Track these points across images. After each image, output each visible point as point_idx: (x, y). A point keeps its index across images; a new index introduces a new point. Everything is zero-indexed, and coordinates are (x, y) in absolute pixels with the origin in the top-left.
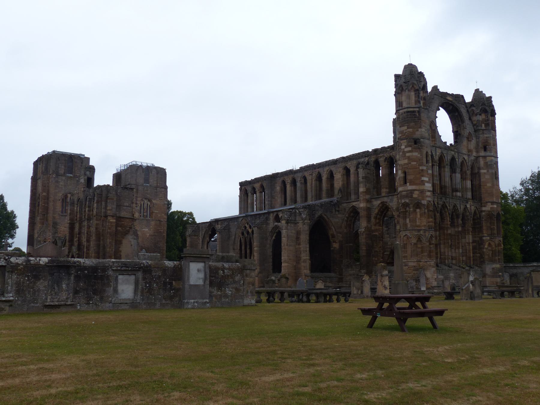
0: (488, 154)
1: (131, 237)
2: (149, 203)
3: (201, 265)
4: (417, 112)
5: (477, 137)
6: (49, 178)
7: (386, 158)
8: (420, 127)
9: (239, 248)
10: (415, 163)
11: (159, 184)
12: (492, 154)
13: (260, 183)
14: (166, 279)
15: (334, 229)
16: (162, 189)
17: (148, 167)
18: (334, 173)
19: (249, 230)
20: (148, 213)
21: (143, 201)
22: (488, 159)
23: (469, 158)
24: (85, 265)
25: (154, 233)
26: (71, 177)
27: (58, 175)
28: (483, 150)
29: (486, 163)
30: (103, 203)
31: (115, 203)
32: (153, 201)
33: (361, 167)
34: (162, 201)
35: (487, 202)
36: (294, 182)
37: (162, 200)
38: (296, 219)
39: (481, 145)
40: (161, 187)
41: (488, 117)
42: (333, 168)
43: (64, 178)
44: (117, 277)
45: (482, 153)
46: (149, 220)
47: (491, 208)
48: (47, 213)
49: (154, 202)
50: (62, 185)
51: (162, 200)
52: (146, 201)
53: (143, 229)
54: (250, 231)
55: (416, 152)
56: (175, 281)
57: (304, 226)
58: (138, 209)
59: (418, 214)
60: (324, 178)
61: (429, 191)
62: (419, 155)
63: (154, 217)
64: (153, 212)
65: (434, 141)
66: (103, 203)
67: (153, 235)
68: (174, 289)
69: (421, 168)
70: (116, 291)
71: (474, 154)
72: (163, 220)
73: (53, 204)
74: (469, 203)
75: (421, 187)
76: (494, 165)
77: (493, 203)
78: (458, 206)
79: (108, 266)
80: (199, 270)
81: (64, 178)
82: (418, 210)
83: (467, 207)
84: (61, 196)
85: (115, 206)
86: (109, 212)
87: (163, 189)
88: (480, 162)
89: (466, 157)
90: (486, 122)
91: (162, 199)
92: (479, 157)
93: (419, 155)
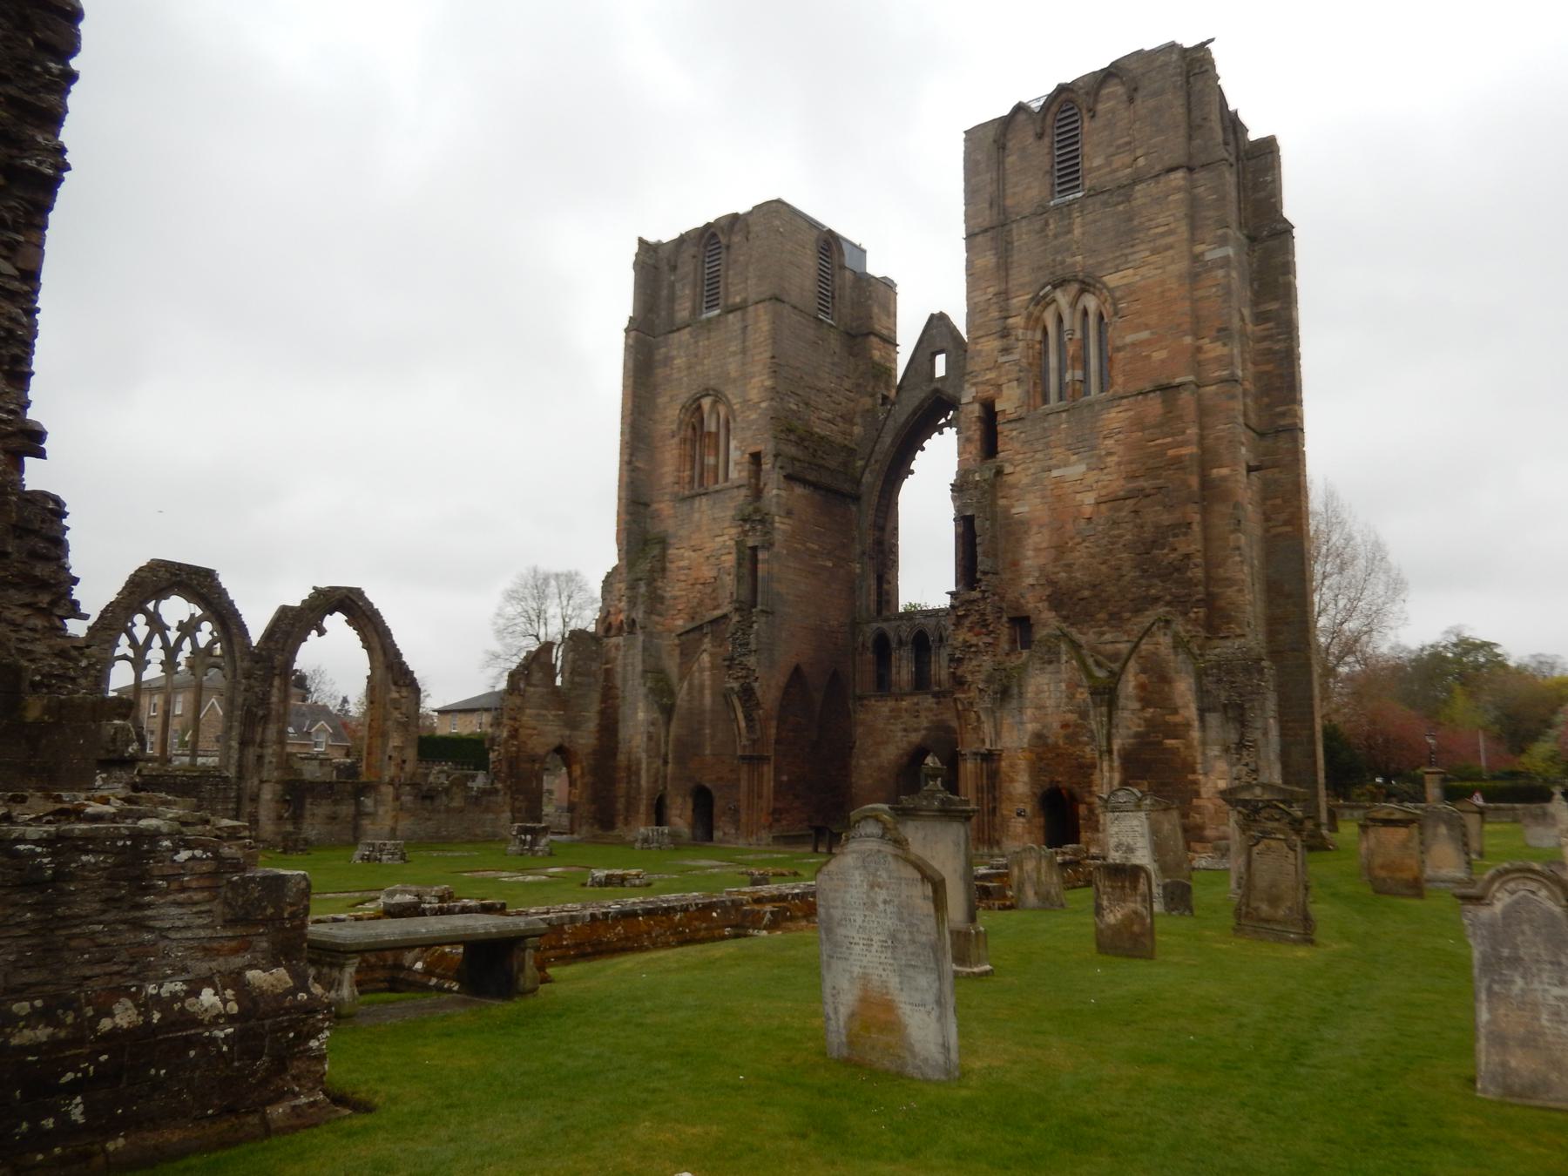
2: (1091, 302)
11: (1145, 155)
16: (1163, 179)
17: (1064, 95)
21: (1052, 308)
26: (709, 320)
32: (1112, 280)
34: (1171, 253)
37: (1169, 247)
40: (1158, 168)
43: (685, 335)
49: (1111, 285)
51: (1169, 247)
52: (1063, 299)
53: (1055, 473)
58: (1016, 362)
63: (1120, 380)
67: (1122, 493)
72: (1191, 378)
81: (688, 336)
87: (1172, 176)
91: (1170, 240)
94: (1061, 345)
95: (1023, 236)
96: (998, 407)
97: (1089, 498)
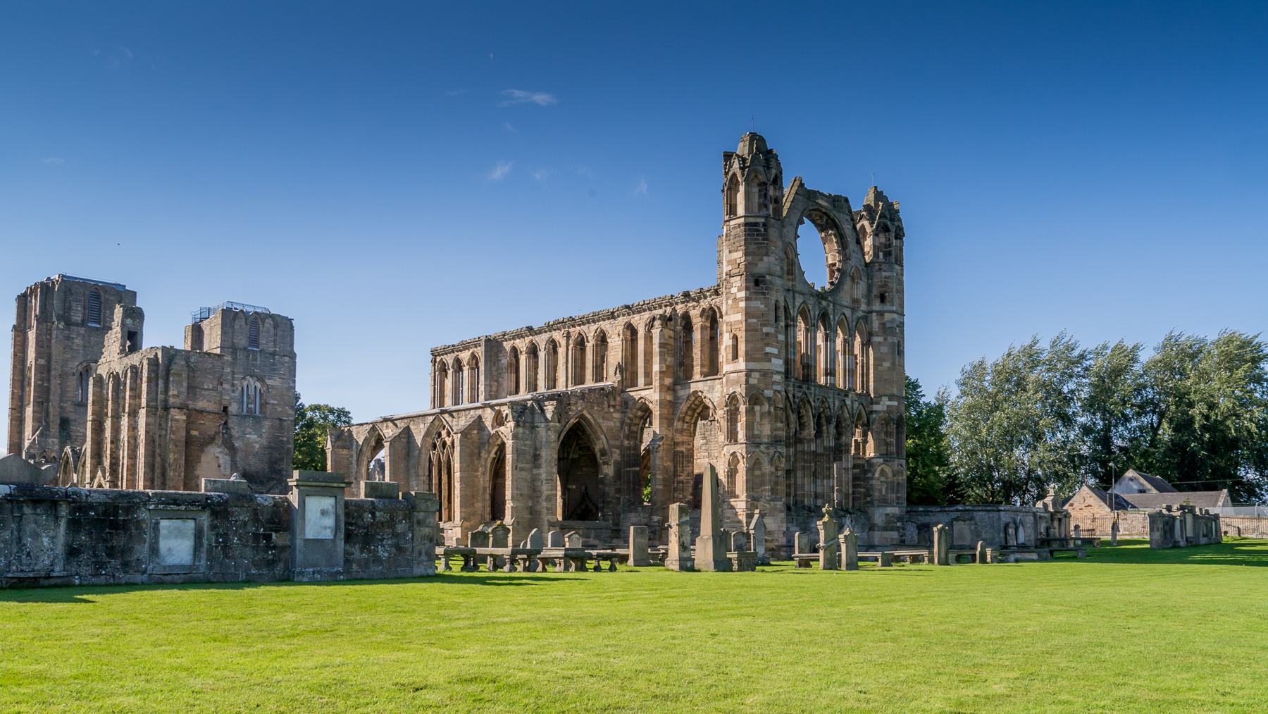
0: (887, 307)
1: (219, 450)
2: (258, 385)
3: (328, 503)
4: (761, 225)
5: (870, 277)
6: (51, 330)
7: (704, 310)
8: (767, 254)
9: (427, 474)
10: (755, 321)
12: (894, 308)
13: (471, 351)
14: (257, 529)
15: (605, 440)
18: (608, 335)
19: (447, 439)
20: (258, 404)
22: (887, 316)
23: (853, 313)
24: (90, 499)
25: (270, 443)
26: (97, 329)
27: (69, 324)
28: (879, 300)
29: (883, 325)
30: (161, 382)
31: (185, 384)
33: (657, 326)
35: (882, 396)
36: (533, 351)
38: (533, 419)
39: (875, 292)
41: (889, 240)
42: (605, 325)
43: (82, 330)
44: (157, 524)
45: (877, 306)
46: (259, 417)
47: (888, 406)
48: (48, 400)
50: (78, 345)
53: (248, 436)
54: (448, 441)
55: (756, 299)
56: (276, 531)
57: (549, 433)
59: (758, 414)
60: (590, 346)
61: (778, 373)
62: (763, 306)
64: (266, 403)
65: (792, 280)
66: (161, 382)
68: (274, 547)
69: (765, 330)
70: (154, 550)
71: (863, 307)
73: (59, 382)
74: (850, 396)
75: (765, 366)
76: (898, 329)
77: (891, 397)
78: (831, 401)
79: (139, 503)
80: (324, 513)
82: (757, 408)
83: (846, 405)
84: (78, 366)
85: (184, 390)
86: (171, 400)
88: (872, 323)
89: (848, 312)
90: (886, 248)
92: (871, 312)
93: (763, 306)
94: (248, 394)
95: (241, 356)
96: (230, 409)
97: (257, 446)
